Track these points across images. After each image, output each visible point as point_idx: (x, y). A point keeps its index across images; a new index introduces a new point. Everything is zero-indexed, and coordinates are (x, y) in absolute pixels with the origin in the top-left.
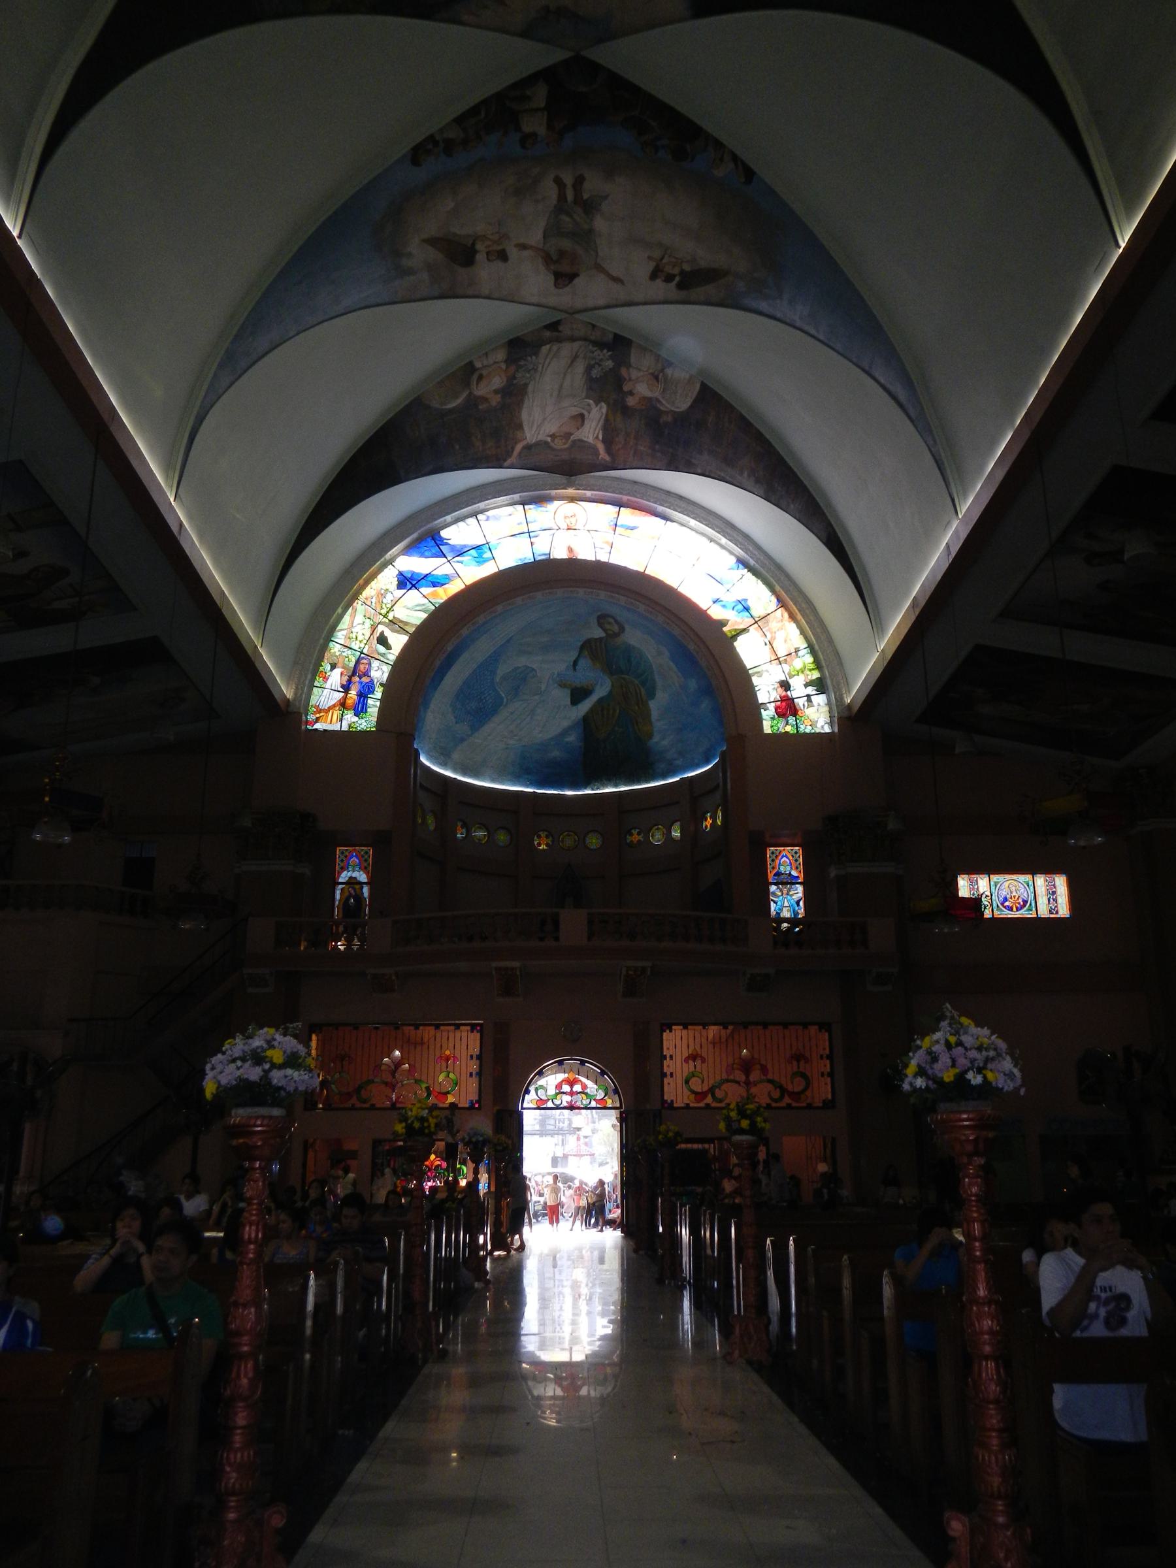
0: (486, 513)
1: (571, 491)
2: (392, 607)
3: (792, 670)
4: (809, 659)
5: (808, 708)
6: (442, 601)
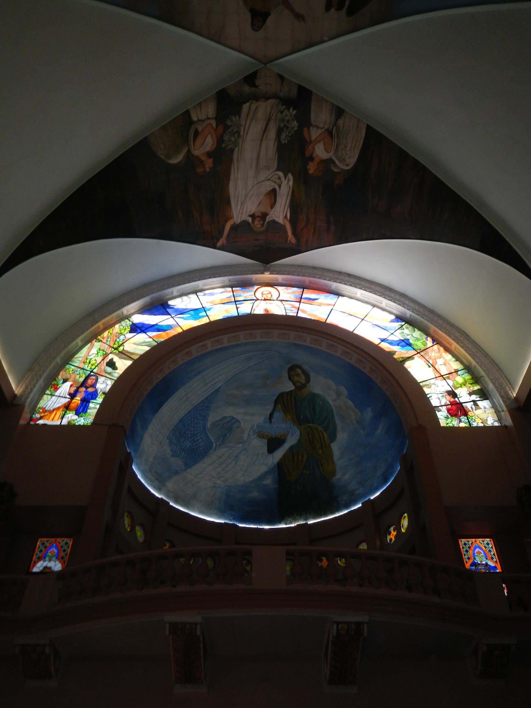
0: (204, 292)
1: (267, 276)
2: (123, 343)
3: (455, 384)
4: (468, 377)
5: (475, 410)
6: (162, 340)
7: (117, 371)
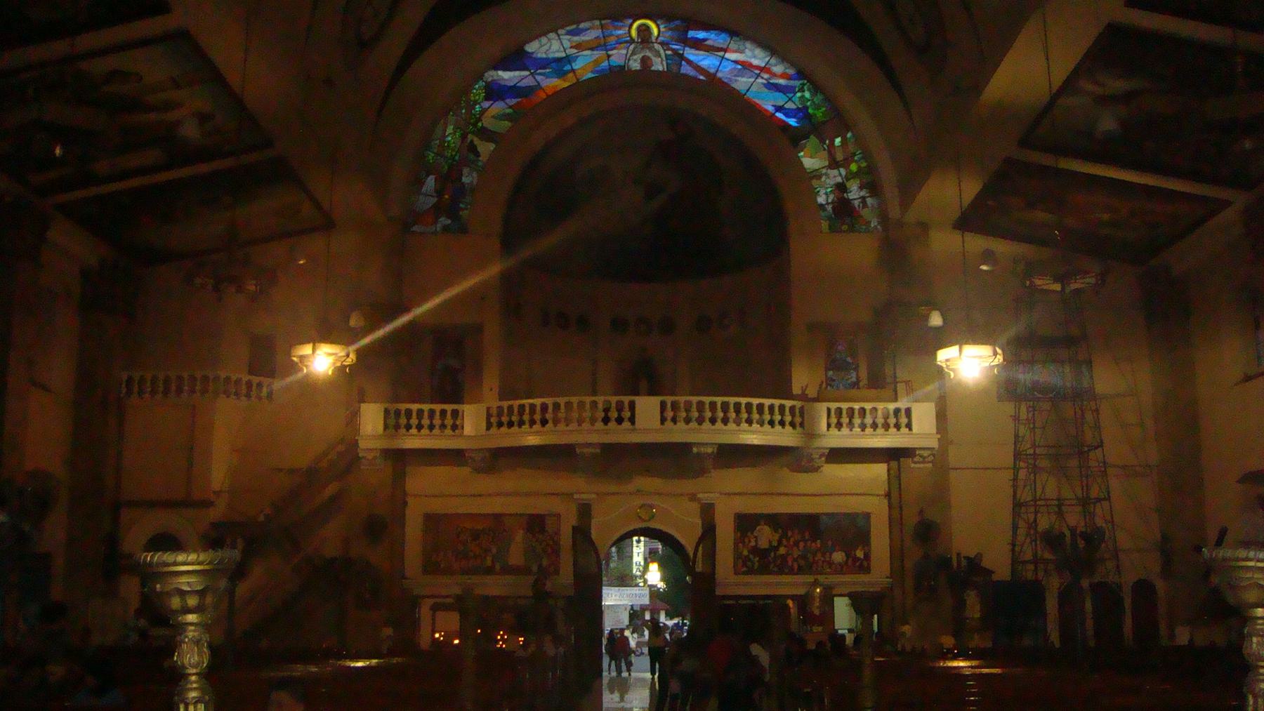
5: (863, 208)
7: (480, 159)
